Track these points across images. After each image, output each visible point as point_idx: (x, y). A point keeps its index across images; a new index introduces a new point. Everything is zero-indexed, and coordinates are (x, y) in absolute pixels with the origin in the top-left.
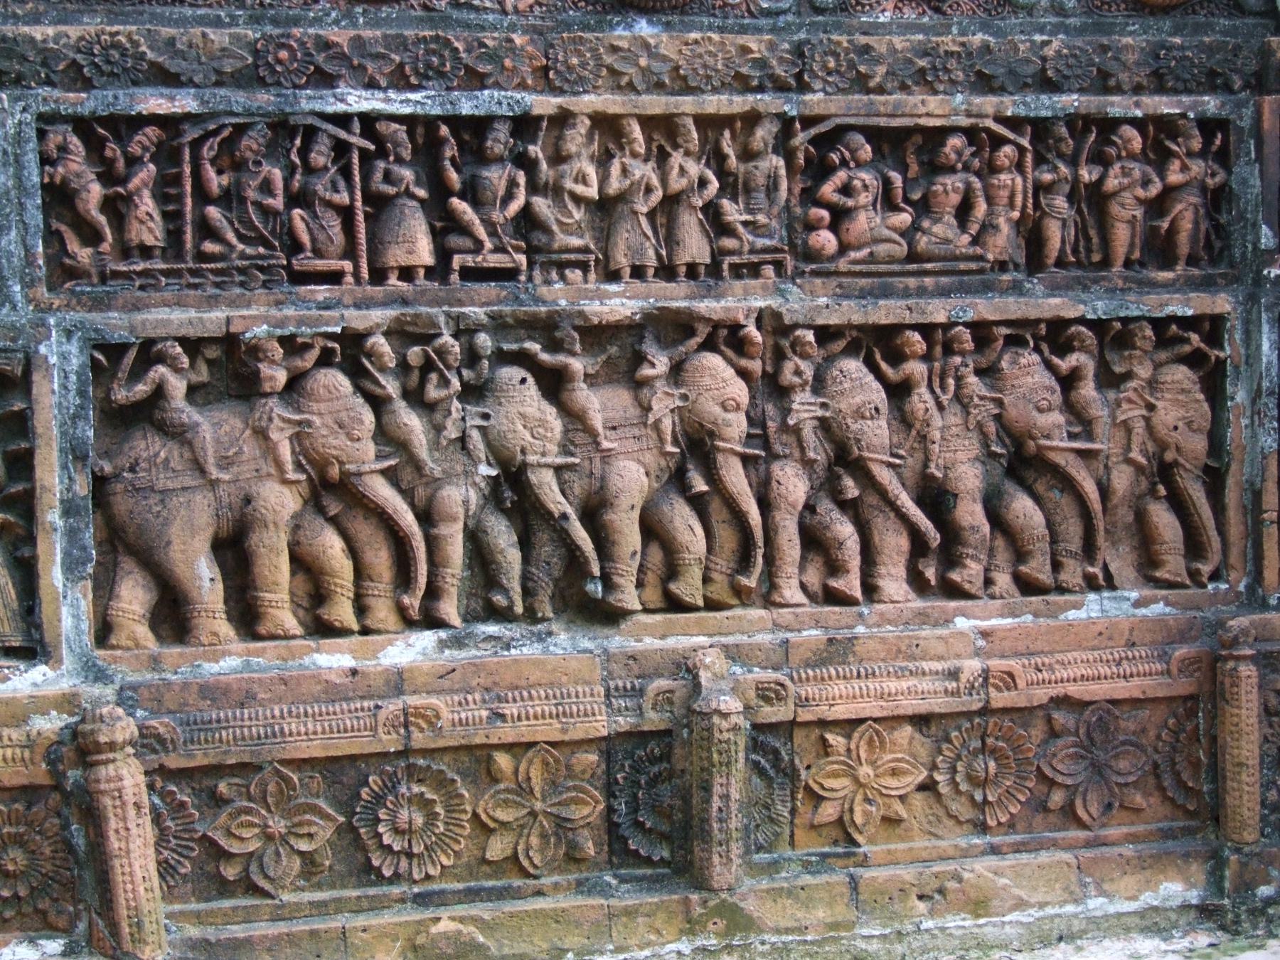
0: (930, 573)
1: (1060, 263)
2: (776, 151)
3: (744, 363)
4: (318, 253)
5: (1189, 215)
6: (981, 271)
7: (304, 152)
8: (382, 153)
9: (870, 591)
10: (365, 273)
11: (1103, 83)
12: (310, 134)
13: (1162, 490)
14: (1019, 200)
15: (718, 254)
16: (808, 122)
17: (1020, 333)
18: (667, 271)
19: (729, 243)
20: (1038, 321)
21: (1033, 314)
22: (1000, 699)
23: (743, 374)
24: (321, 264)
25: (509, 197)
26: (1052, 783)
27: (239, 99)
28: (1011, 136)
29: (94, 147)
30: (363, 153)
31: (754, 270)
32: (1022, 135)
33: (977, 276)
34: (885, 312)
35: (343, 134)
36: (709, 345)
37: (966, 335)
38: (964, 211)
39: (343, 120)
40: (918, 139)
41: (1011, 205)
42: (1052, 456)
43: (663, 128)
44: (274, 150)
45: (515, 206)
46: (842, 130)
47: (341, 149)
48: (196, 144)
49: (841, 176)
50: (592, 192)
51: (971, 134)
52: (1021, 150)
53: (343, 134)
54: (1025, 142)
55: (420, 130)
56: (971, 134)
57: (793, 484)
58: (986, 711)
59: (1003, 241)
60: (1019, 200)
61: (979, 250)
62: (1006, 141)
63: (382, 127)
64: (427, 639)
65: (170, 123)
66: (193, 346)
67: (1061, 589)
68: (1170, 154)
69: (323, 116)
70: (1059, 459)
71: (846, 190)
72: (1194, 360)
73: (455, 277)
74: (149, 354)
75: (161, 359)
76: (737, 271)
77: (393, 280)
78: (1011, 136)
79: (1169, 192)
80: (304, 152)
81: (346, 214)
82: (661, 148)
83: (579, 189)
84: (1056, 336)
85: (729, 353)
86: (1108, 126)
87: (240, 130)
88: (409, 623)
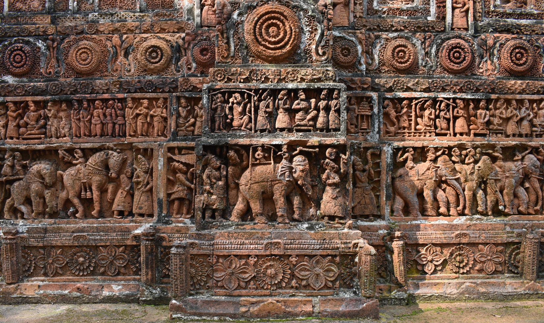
4: (442, 129)
7: (440, 106)
8: (456, 107)
10: (452, 134)
12: (441, 102)
15: (532, 131)
18: (520, 135)
23: (538, 159)
24: (443, 131)
25: (485, 117)
27: (426, 95)
29: (394, 104)
30: (453, 106)
35: (448, 102)
36: (530, 153)
39: (448, 99)
43: (521, 102)
44: (433, 105)
45: (486, 119)
47: (448, 105)
48: (416, 104)
50: (504, 116)
53: (448, 102)
55: (466, 102)
63: (458, 101)
64: (464, 218)
65: (411, 100)
66: (415, 149)
69: (444, 98)
73: (472, 135)
74: (405, 150)
75: (408, 152)
76: (537, 136)
77: (458, 135)
80: (440, 106)
81: (448, 120)
82: (520, 107)
83: (501, 116)
87: (426, 101)
88: (460, 215)
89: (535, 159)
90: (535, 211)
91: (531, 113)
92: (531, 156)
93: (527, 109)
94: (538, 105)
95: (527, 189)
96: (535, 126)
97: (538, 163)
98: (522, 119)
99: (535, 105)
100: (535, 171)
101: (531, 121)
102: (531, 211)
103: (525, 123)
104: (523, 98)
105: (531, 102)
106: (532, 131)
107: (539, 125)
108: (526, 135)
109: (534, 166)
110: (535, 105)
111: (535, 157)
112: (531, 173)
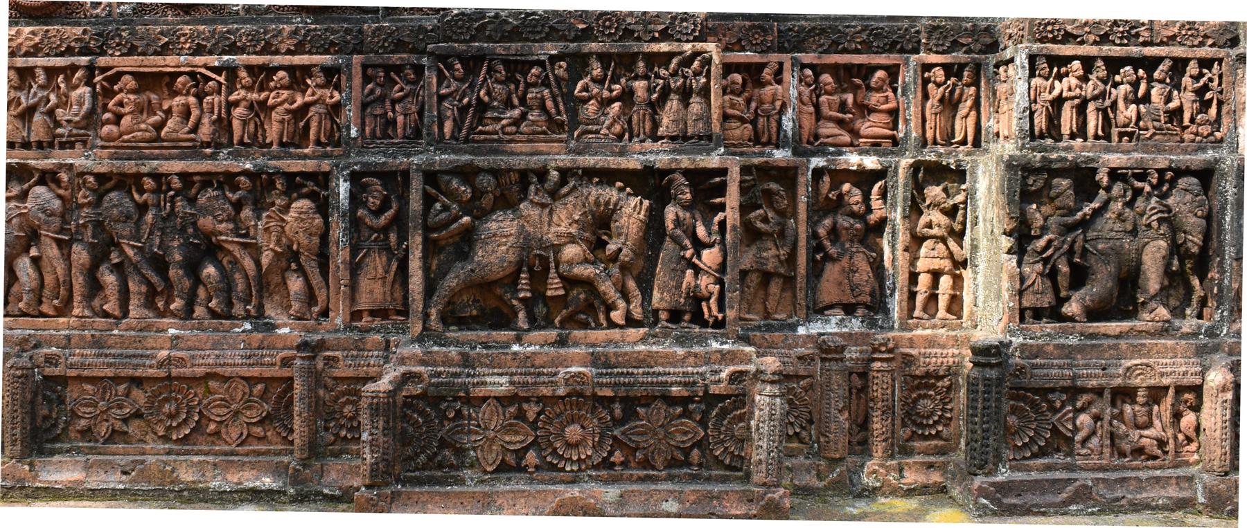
0: (160, 304)
1: (241, 143)
2: (87, 84)
3: (61, 192)
5: (316, 118)
6: (195, 147)
9: (125, 314)
11: (267, 49)
13: (293, 266)
14: (216, 111)
16: (104, 70)
17: (208, 179)
19: (60, 131)
20: (217, 174)
21: (213, 169)
22: (175, 372)
23: (60, 197)
26: (210, 420)
28: (214, 76)
31: (71, 145)
32: (220, 75)
33: (194, 150)
34: (130, 167)
36: (42, 182)
37: (176, 179)
38: (186, 113)
40: (167, 79)
41: (212, 112)
42: (226, 245)
46: (120, 75)
49: (119, 96)
51: (192, 75)
52: (220, 84)
54: (222, 79)
56: (192, 75)
57: (80, 254)
58: (169, 378)
59: (206, 131)
60: (216, 111)
61: (193, 135)
62: (212, 79)
67: (229, 317)
68: (308, 86)
70: (230, 247)
71: (121, 104)
72: (312, 196)
76: (63, 146)
78: (214, 76)
79: (306, 107)
84: (228, 180)
85: (53, 186)
86: (271, 71)
89: (48, 195)
90: (56, 308)
91: (53, 97)
92: (40, 190)
93: (42, 87)
94: (68, 80)
95: (36, 261)
96: (58, 124)
97: (57, 204)
98: (31, 110)
99: (61, 78)
100: (47, 223)
101: (51, 113)
102: (45, 308)
103: (38, 118)
104: (30, 64)
105: (51, 72)
106: (55, 136)
107: (69, 121)
108: (40, 145)
109: (44, 211)
110: (61, 78)
111: (51, 190)
112: (39, 227)
